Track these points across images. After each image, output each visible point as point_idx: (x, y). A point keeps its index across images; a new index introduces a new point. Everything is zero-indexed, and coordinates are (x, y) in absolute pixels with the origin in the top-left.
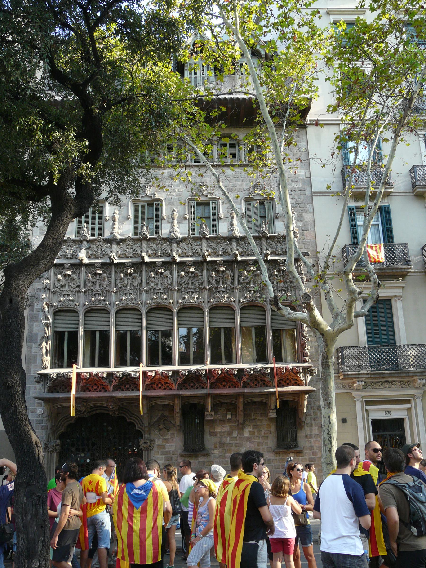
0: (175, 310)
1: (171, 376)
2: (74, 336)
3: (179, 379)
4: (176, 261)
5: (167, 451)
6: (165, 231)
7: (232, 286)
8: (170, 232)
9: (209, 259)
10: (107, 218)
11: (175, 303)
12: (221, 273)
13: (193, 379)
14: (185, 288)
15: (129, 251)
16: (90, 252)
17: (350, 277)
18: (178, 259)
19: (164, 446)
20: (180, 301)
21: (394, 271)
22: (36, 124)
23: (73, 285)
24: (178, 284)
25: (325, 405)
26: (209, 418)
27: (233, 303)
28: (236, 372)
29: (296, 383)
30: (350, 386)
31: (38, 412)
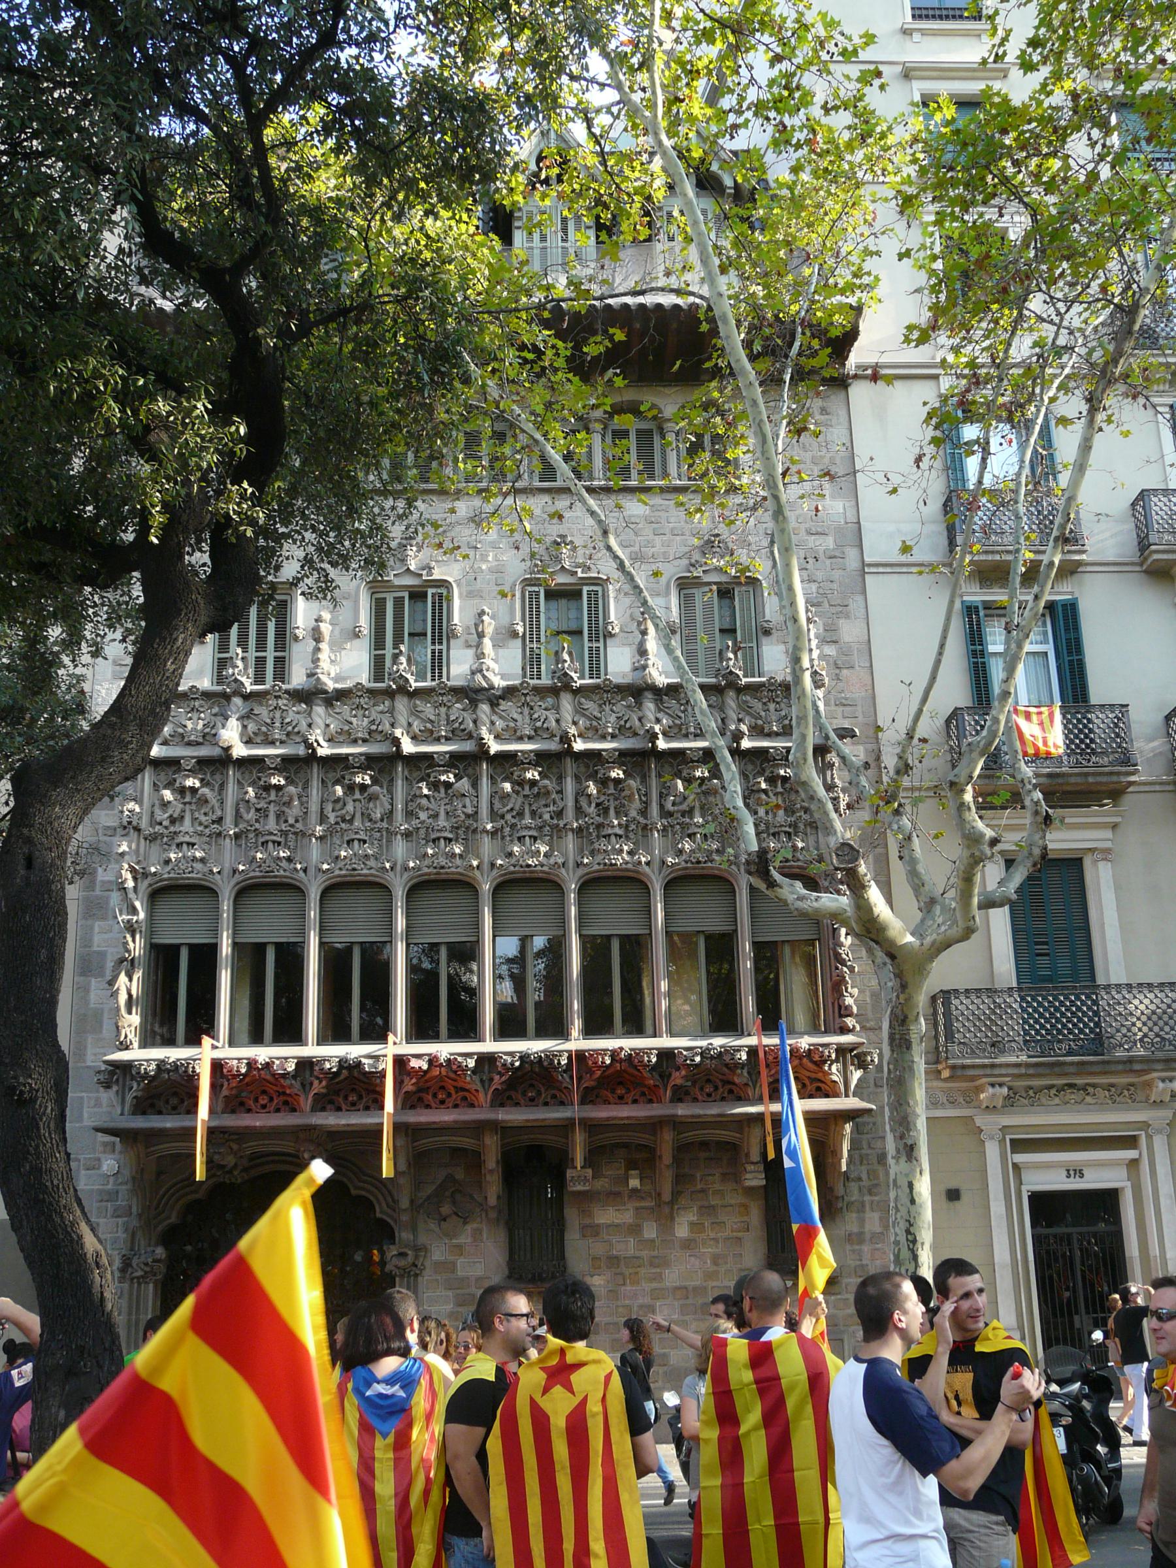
0: (486, 887)
1: (475, 1071)
2: (205, 957)
3: (497, 1077)
4: (487, 752)
5: (463, 1279)
6: (459, 668)
7: (642, 820)
8: (473, 673)
9: (579, 746)
10: (300, 633)
11: (486, 866)
12: (611, 785)
13: (534, 1078)
14: (513, 826)
15: (360, 724)
16: (252, 727)
17: (968, 797)
18: (494, 747)
19: (454, 1264)
20: (499, 862)
21: (1091, 779)
22: (102, 376)
23: (203, 818)
24: (494, 815)
25: (898, 1151)
26: (579, 1188)
27: (647, 869)
28: (654, 1060)
29: (819, 1089)
30: (970, 1097)
31: (105, 1168)
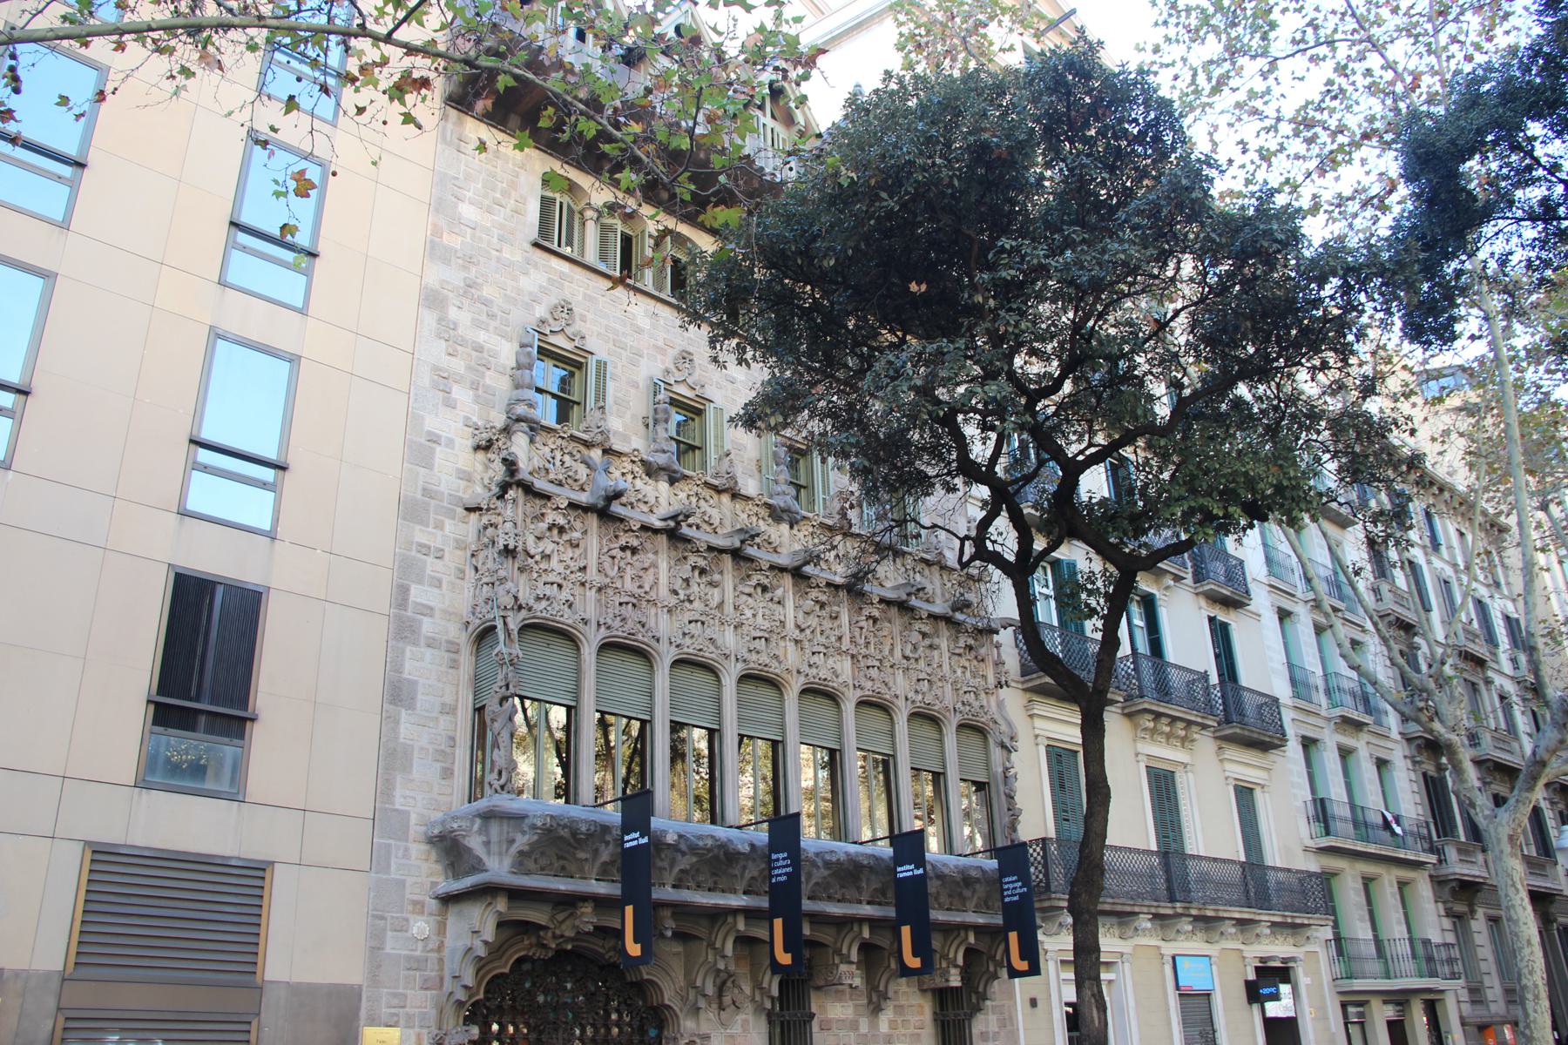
31: (415, 931)
